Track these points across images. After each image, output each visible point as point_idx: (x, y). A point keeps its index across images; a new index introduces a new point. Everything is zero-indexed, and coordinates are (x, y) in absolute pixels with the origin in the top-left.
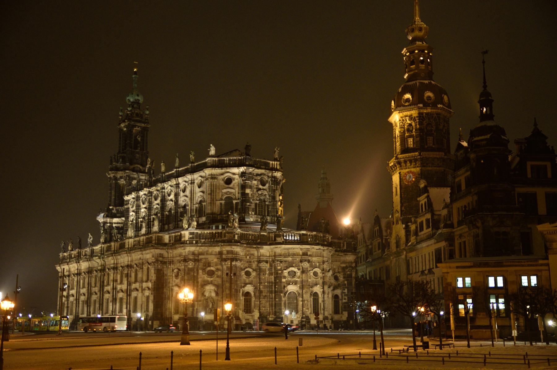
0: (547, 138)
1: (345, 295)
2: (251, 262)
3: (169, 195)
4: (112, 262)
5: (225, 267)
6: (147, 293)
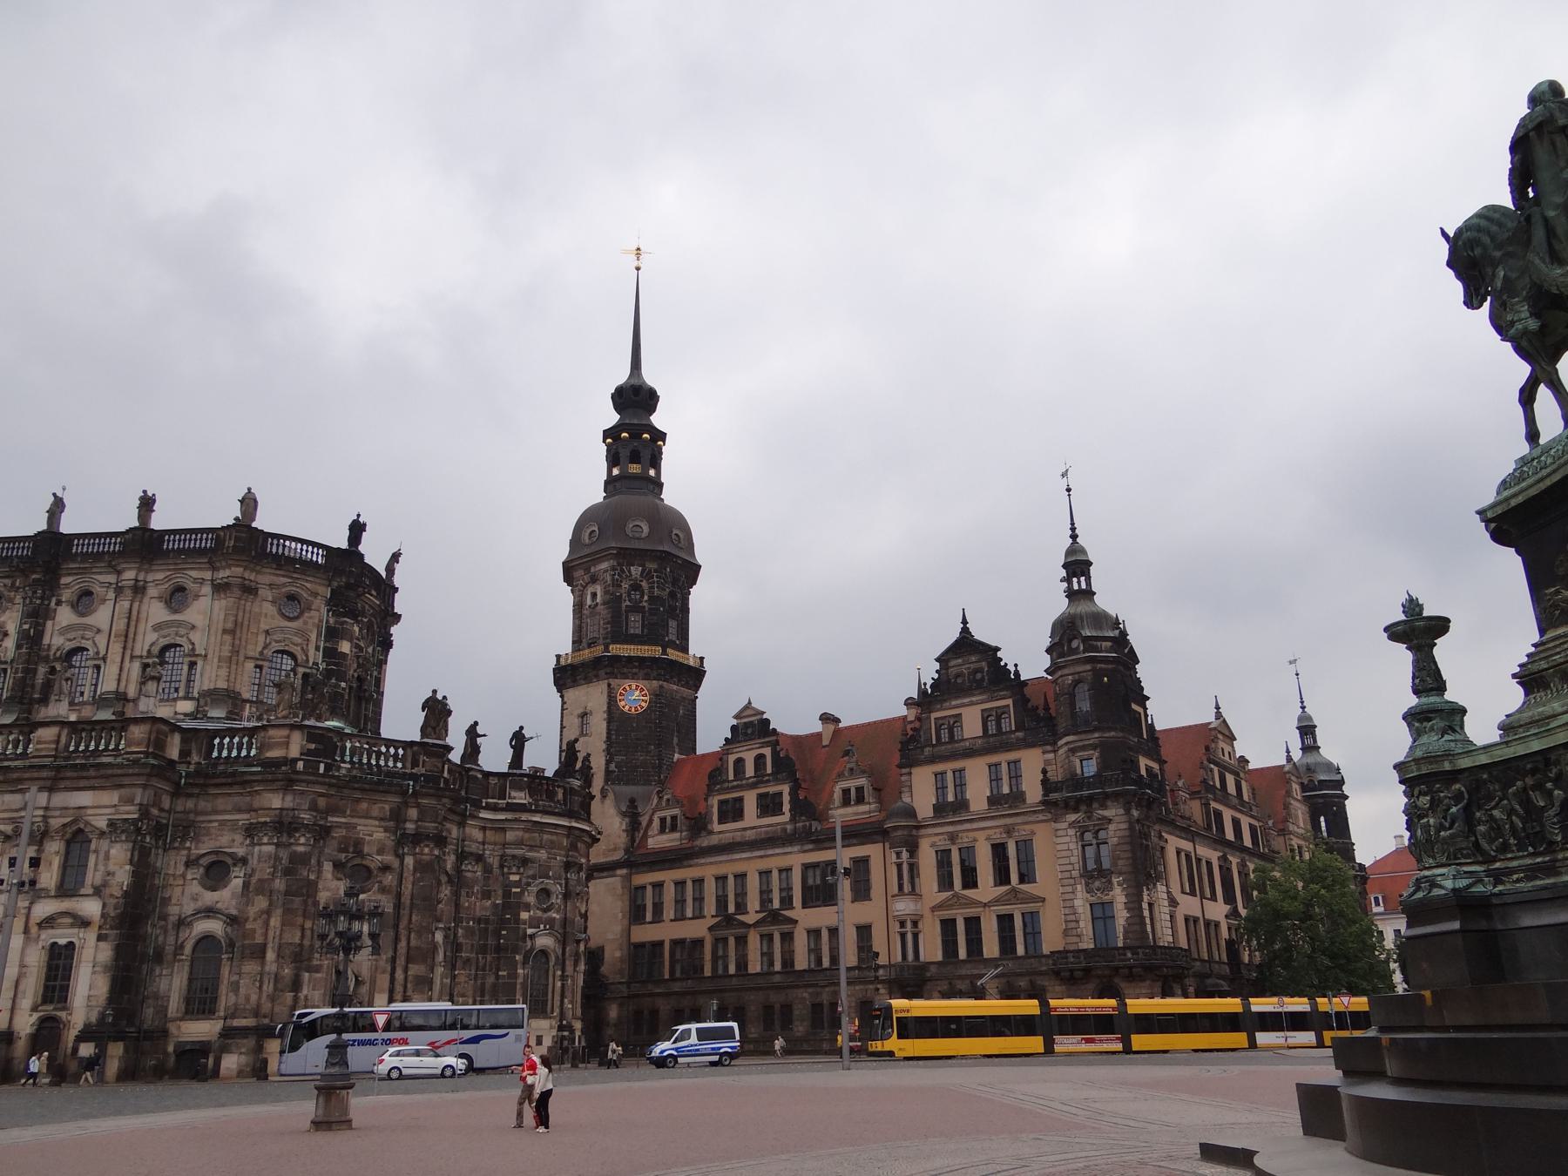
5: (409, 861)
6: (62, 937)
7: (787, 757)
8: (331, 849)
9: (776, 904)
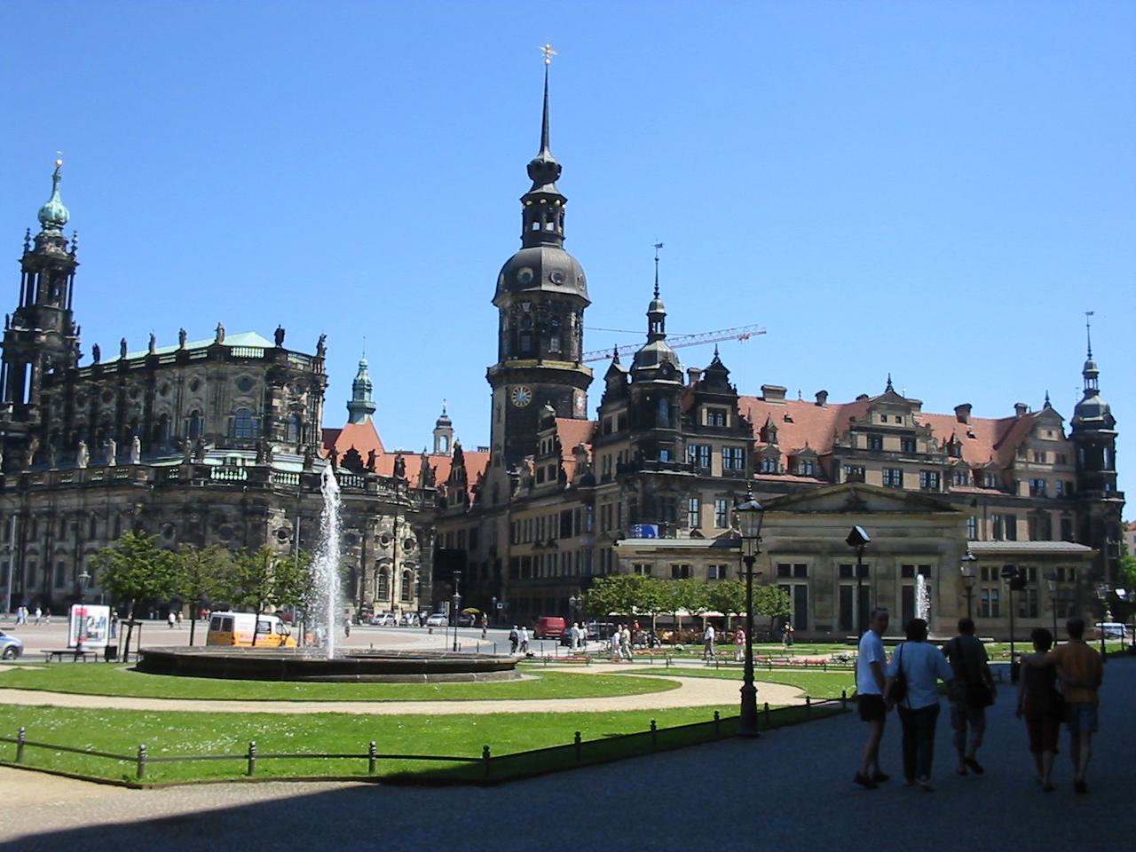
0: (728, 372)
3: (134, 396)
4: (46, 503)
5: (250, 525)
7: (559, 442)
9: (553, 537)
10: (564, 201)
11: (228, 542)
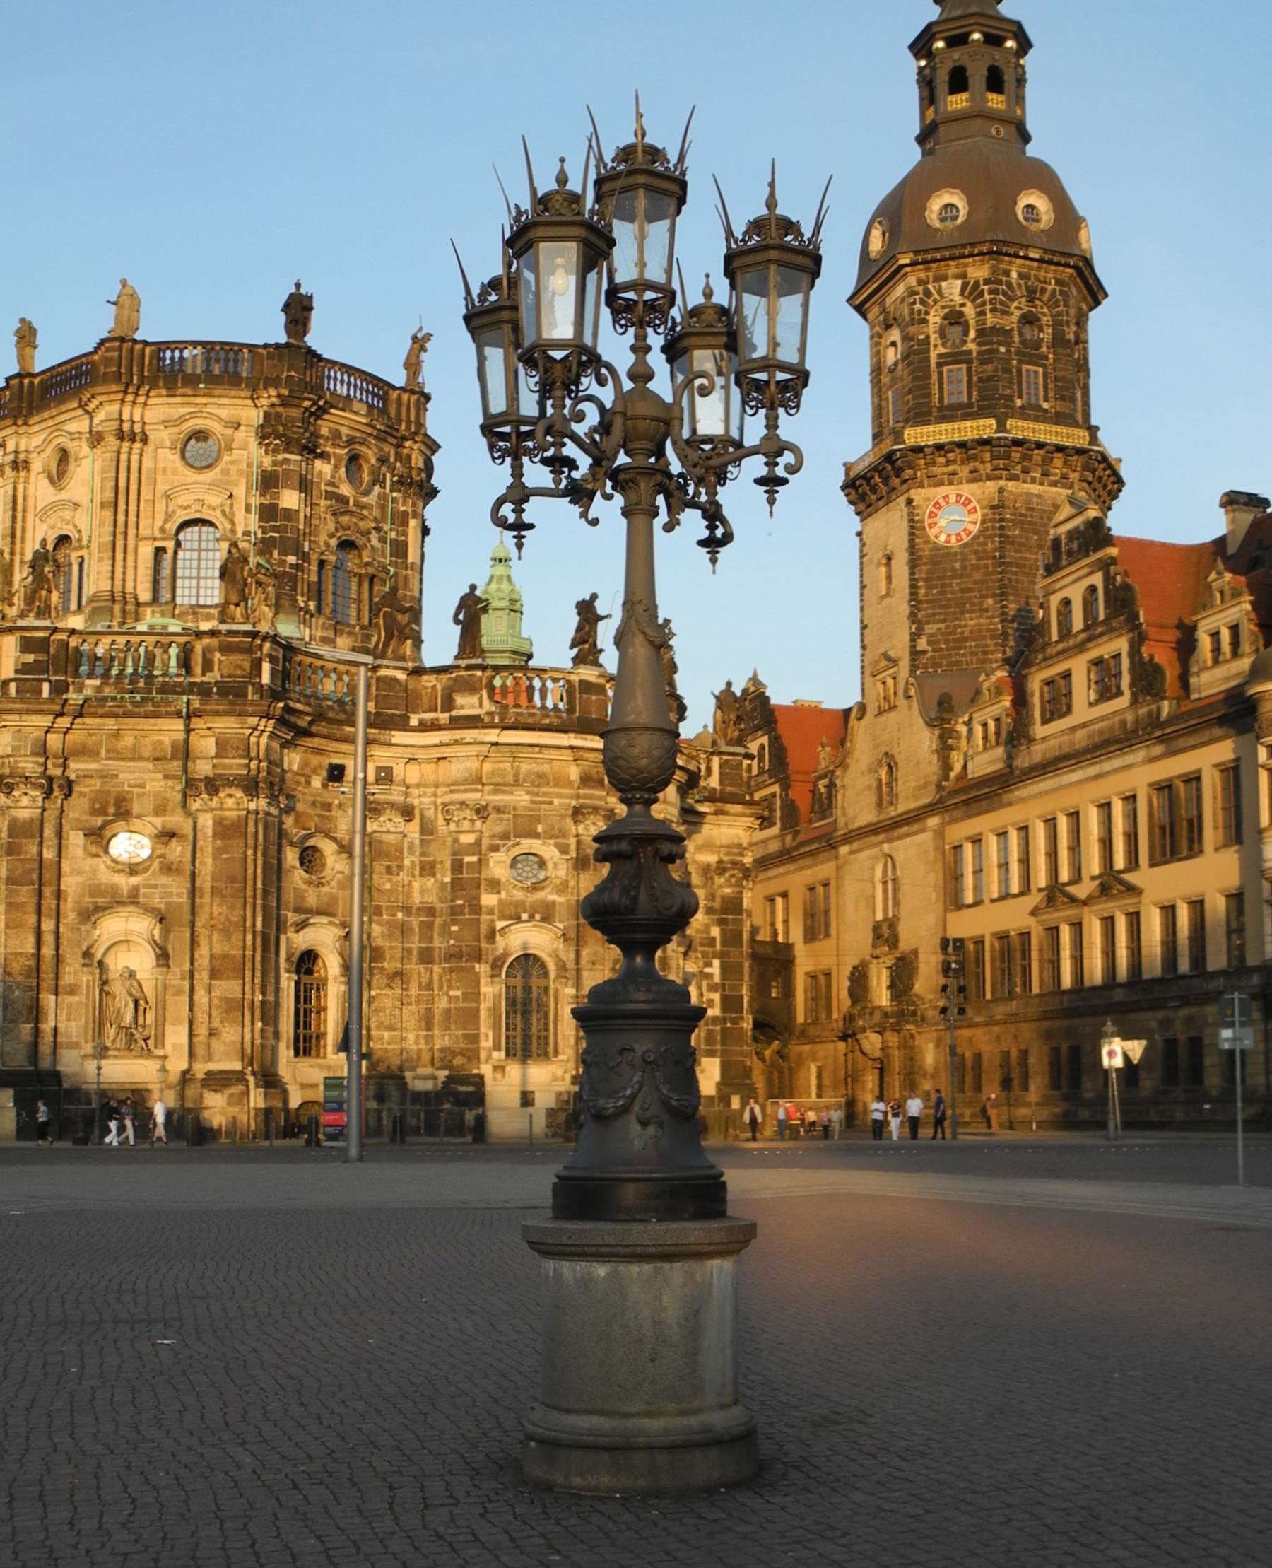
1: (712, 988)
2: (327, 806)
5: (206, 822)
8: (78, 808)
9: (1120, 862)
10: (1025, 44)
11: (134, 880)
